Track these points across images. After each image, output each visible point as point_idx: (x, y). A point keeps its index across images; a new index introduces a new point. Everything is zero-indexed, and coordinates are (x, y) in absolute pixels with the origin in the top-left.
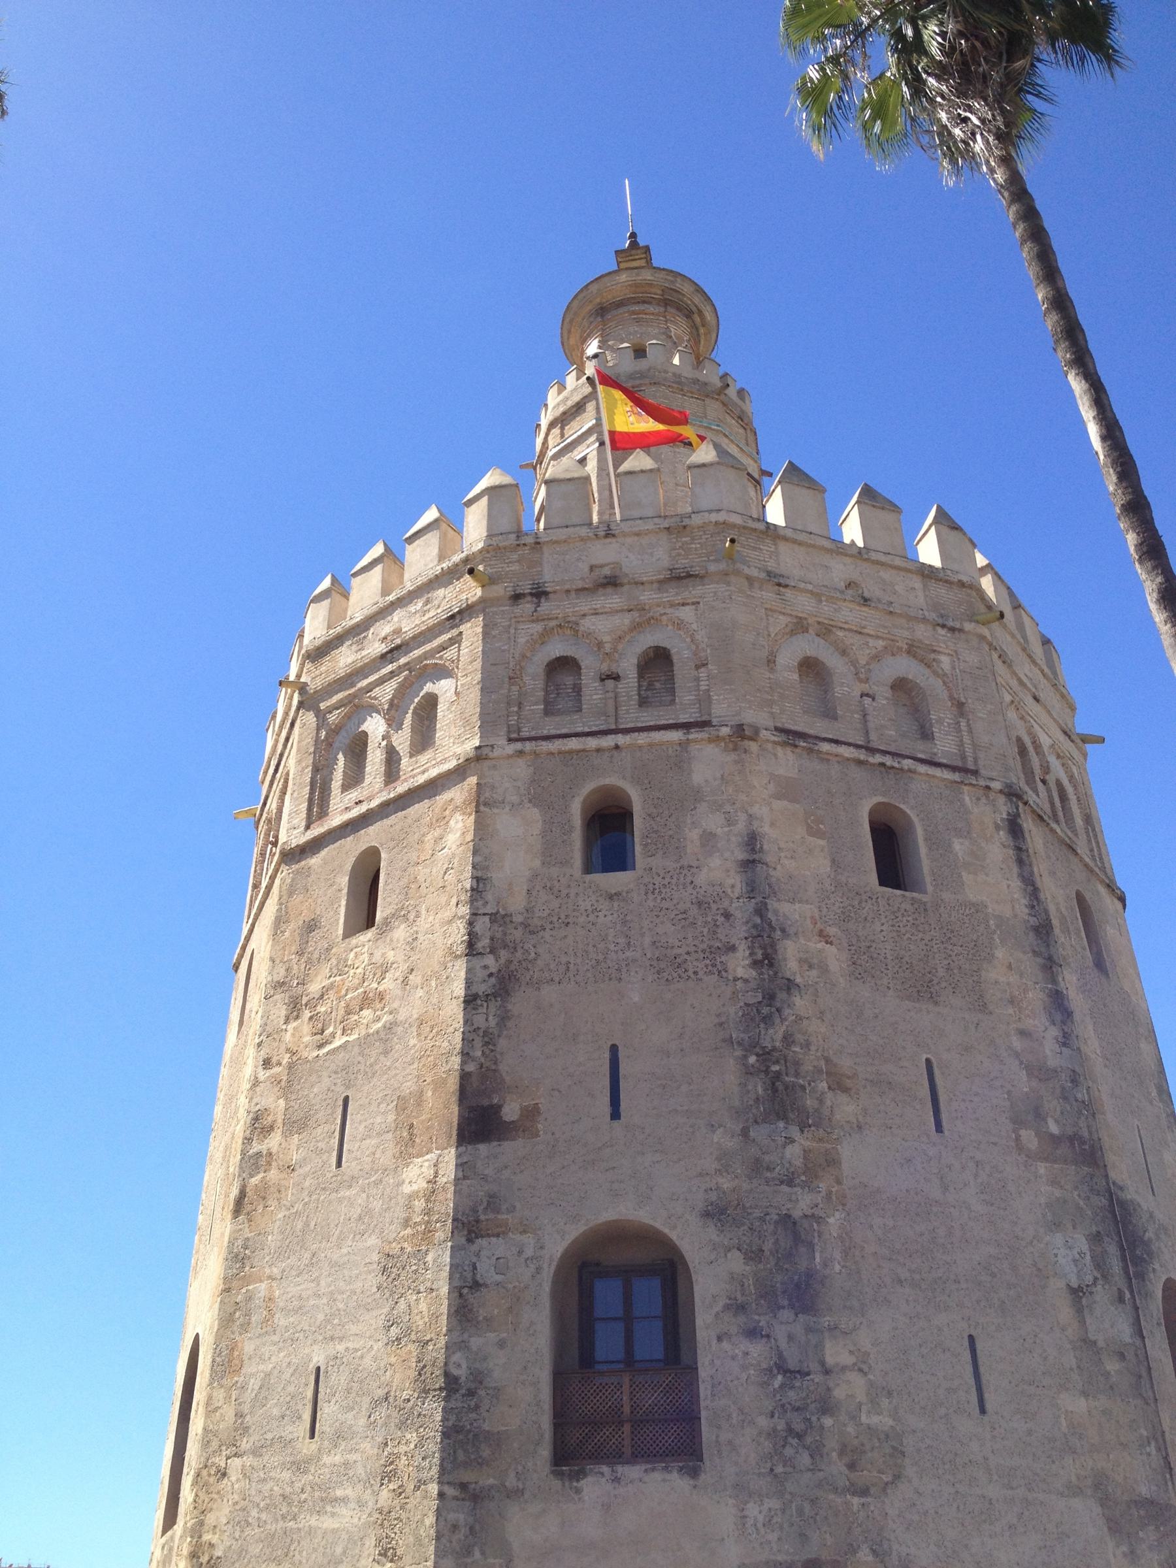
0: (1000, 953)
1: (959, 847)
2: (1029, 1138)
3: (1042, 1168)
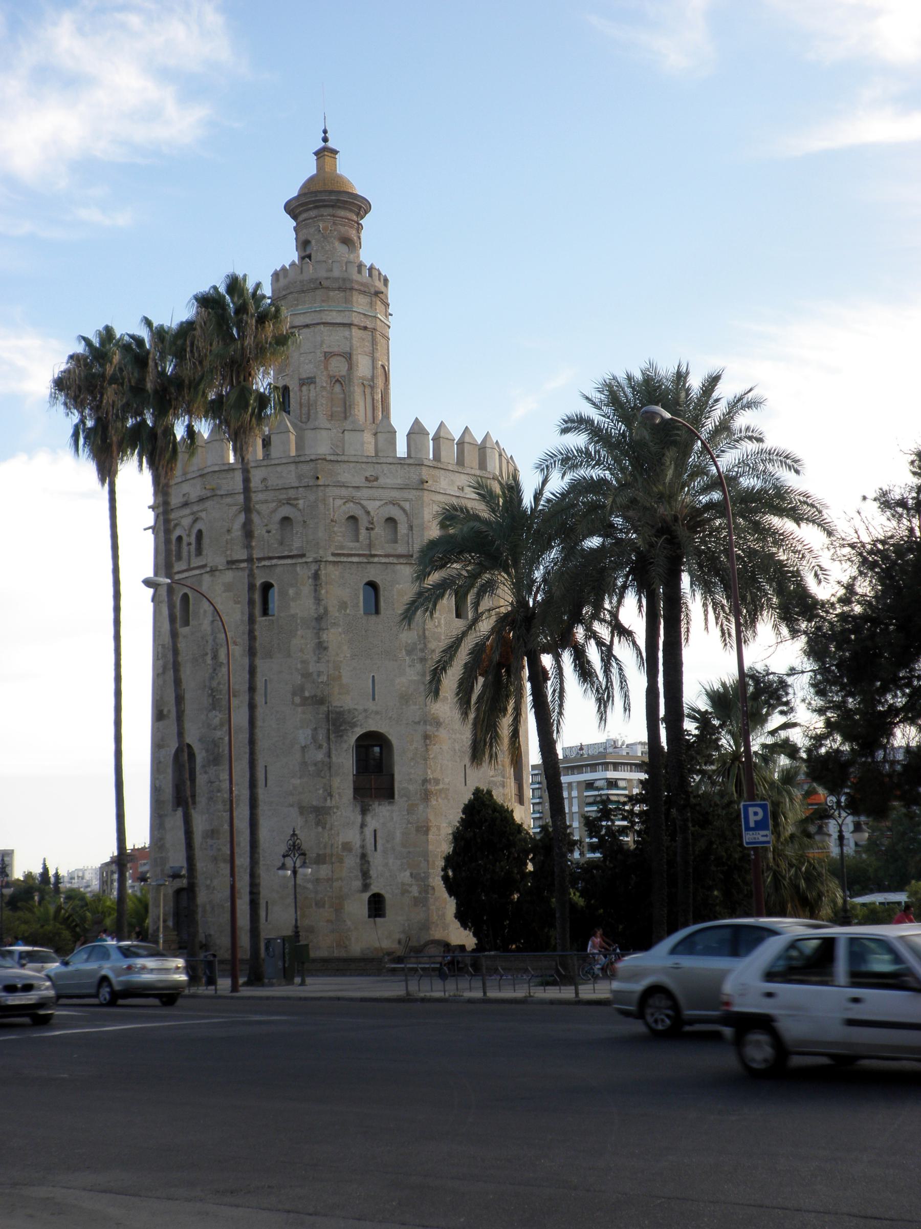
0: (299, 633)
1: (291, 592)
2: (297, 700)
3: (300, 709)
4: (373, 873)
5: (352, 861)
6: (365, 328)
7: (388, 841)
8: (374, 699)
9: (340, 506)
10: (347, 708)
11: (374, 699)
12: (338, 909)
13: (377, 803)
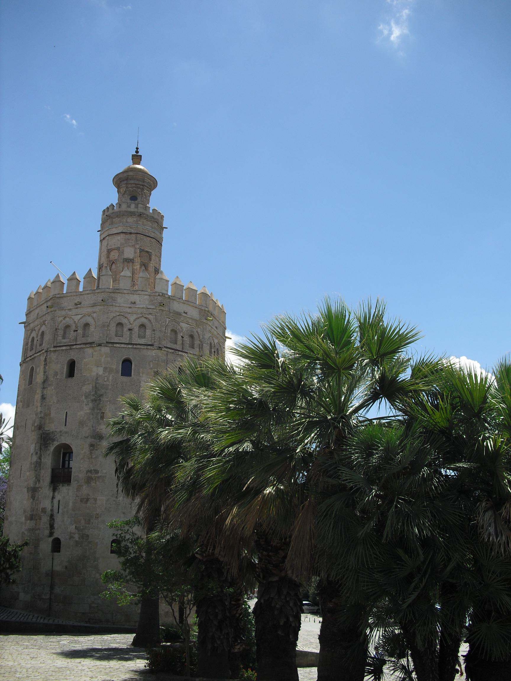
4: (56, 526)
5: (45, 519)
6: (131, 233)
7: (65, 507)
8: (66, 425)
9: (62, 321)
10: (51, 431)
11: (66, 425)
12: (36, 546)
13: (61, 485)
